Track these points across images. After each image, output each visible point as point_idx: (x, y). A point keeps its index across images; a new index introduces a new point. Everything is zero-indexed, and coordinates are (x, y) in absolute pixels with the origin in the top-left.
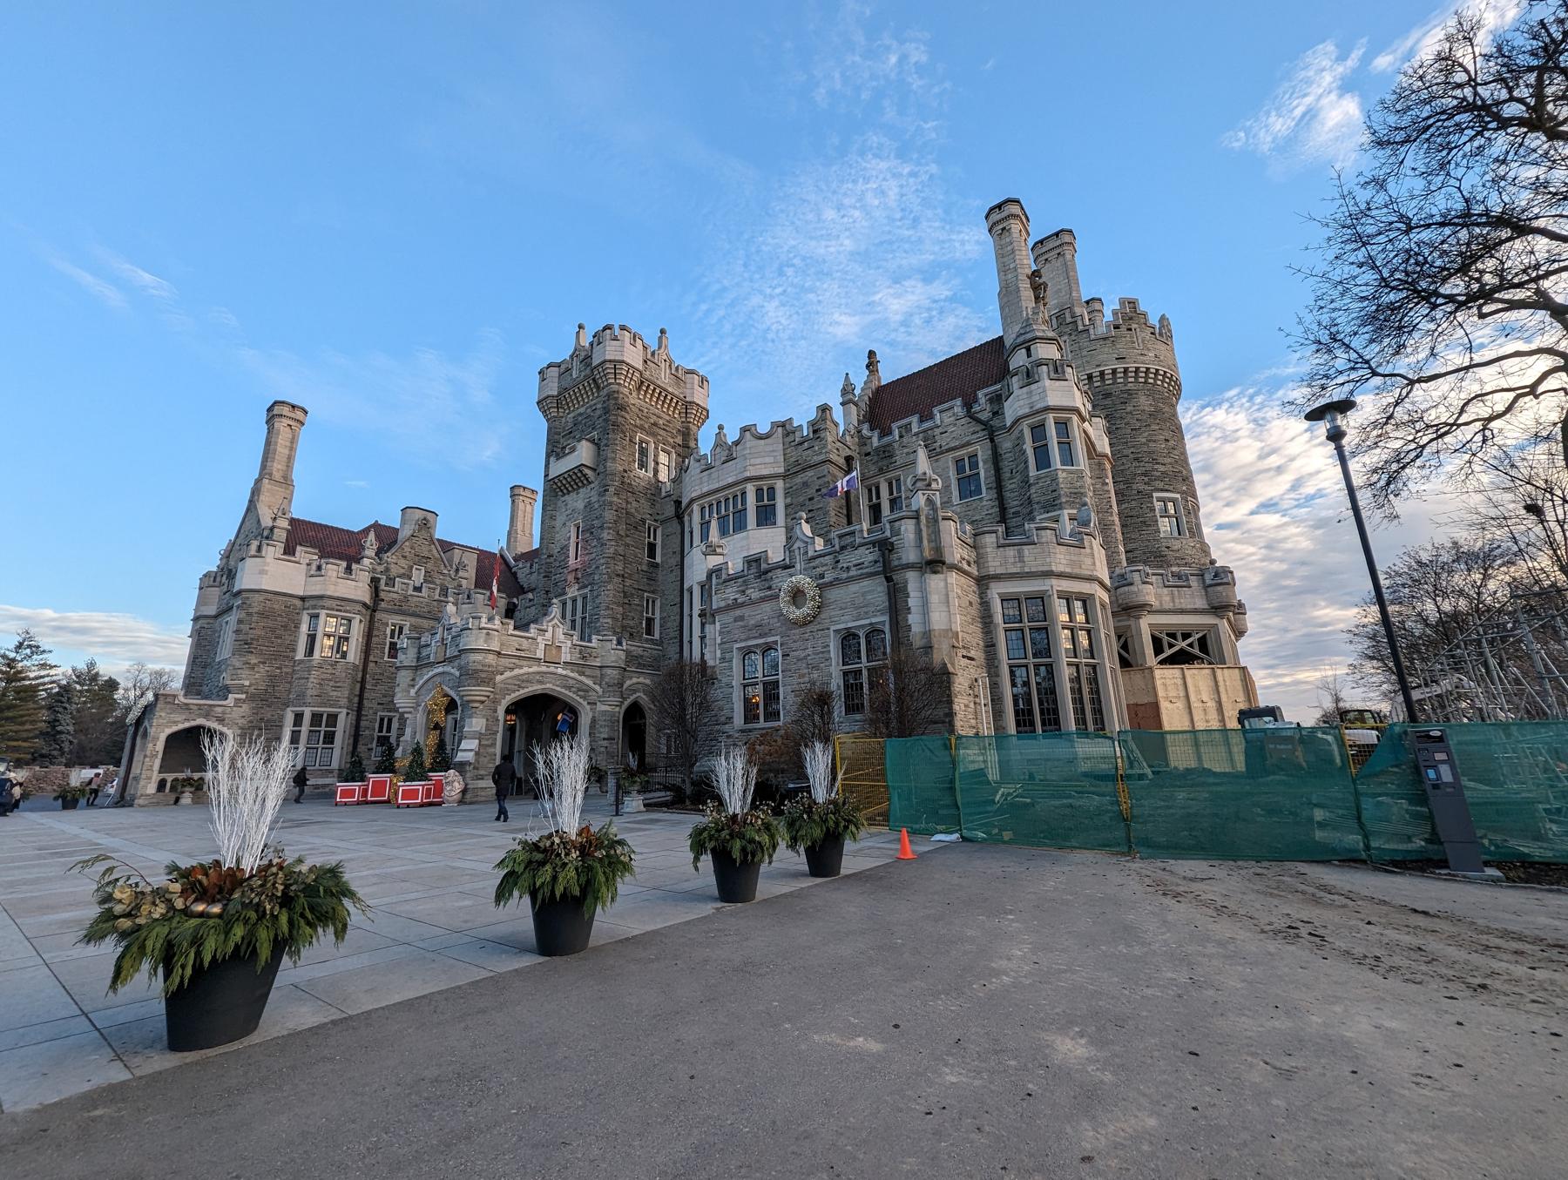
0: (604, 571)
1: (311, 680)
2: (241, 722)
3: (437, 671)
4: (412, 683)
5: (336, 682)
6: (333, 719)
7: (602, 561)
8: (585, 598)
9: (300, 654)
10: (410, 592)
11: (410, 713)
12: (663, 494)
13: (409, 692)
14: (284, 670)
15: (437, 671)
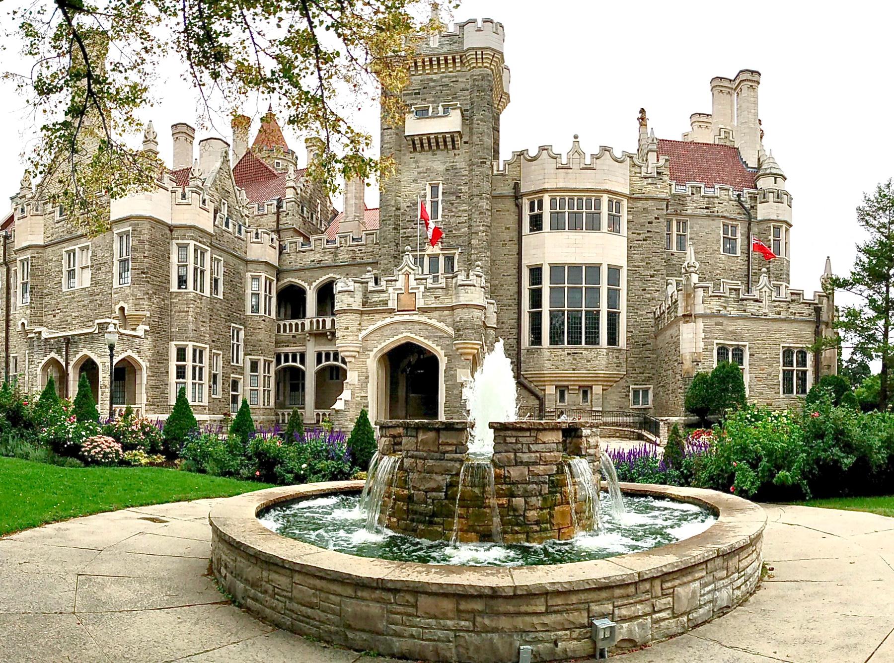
0: (484, 238)
1: (191, 313)
2: (148, 354)
3: (397, 318)
4: (359, 327)
5: (203, 317)
6: (201, 352)
7: (481, 228)
8: (450, 259)
9: (174, 287)
10: (224, 228)
11: (355, 357)
12: (495, 172)
13: (357, 336)
14: (166, 302)
15: (397, 318)
